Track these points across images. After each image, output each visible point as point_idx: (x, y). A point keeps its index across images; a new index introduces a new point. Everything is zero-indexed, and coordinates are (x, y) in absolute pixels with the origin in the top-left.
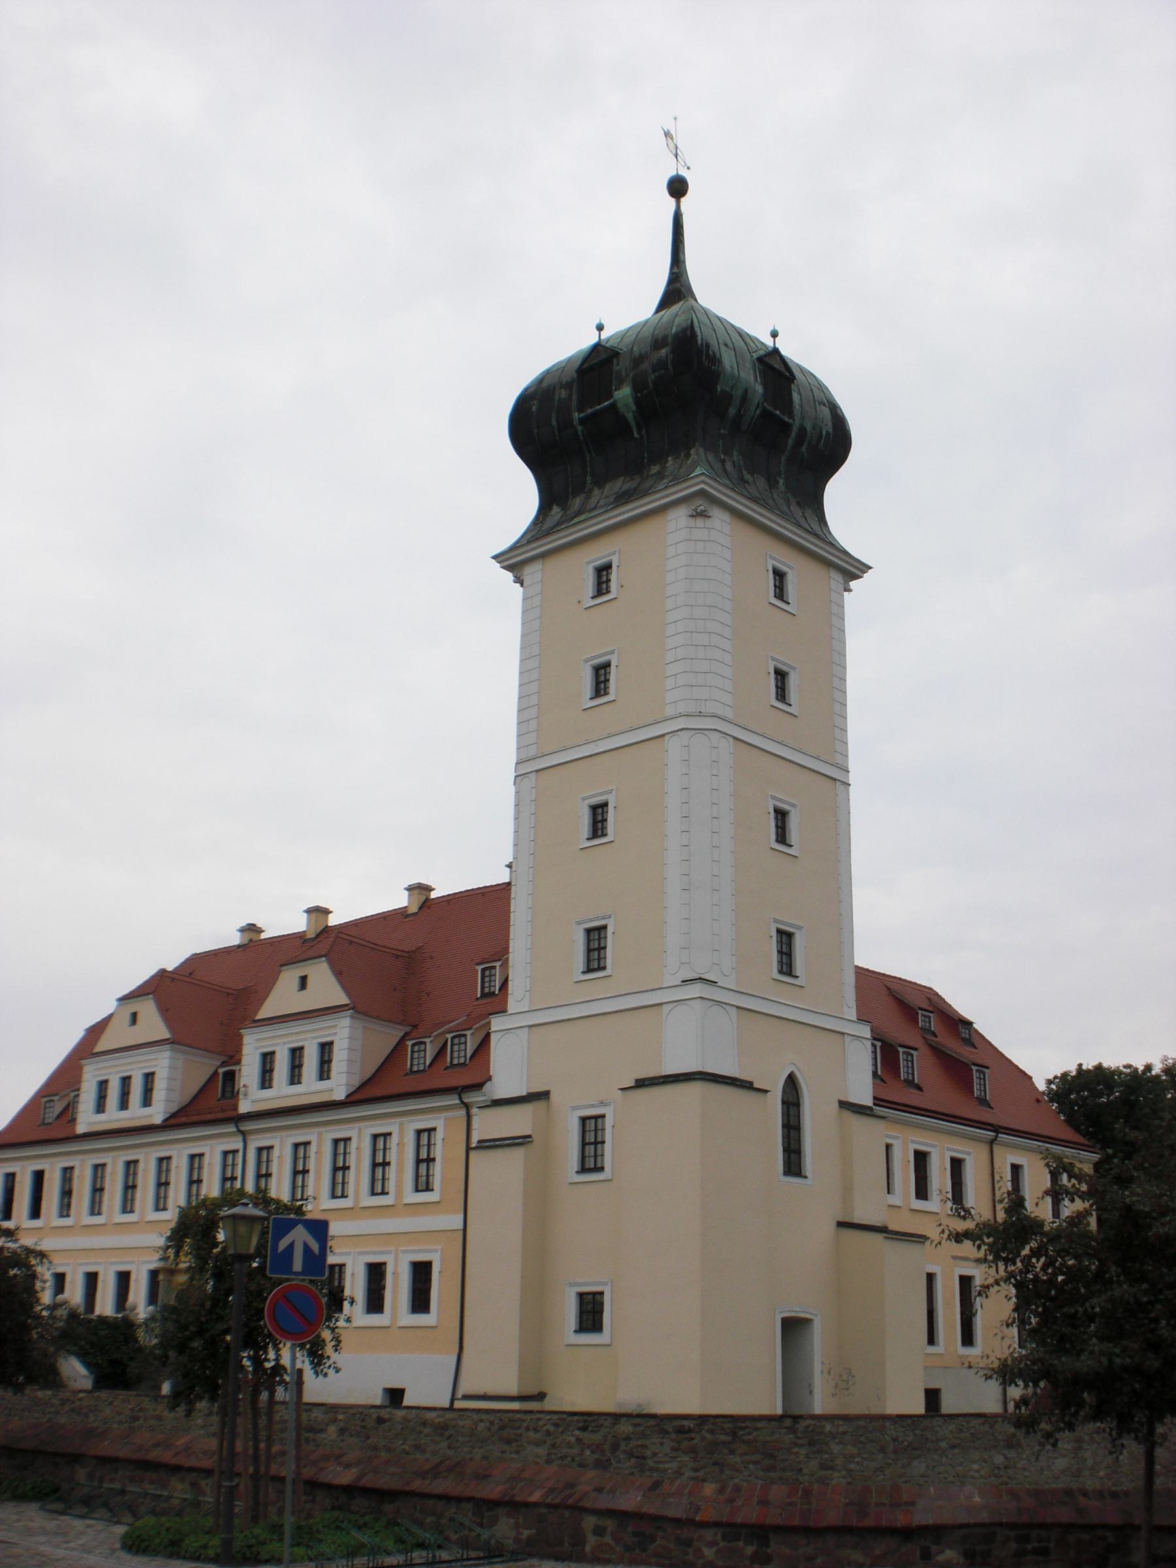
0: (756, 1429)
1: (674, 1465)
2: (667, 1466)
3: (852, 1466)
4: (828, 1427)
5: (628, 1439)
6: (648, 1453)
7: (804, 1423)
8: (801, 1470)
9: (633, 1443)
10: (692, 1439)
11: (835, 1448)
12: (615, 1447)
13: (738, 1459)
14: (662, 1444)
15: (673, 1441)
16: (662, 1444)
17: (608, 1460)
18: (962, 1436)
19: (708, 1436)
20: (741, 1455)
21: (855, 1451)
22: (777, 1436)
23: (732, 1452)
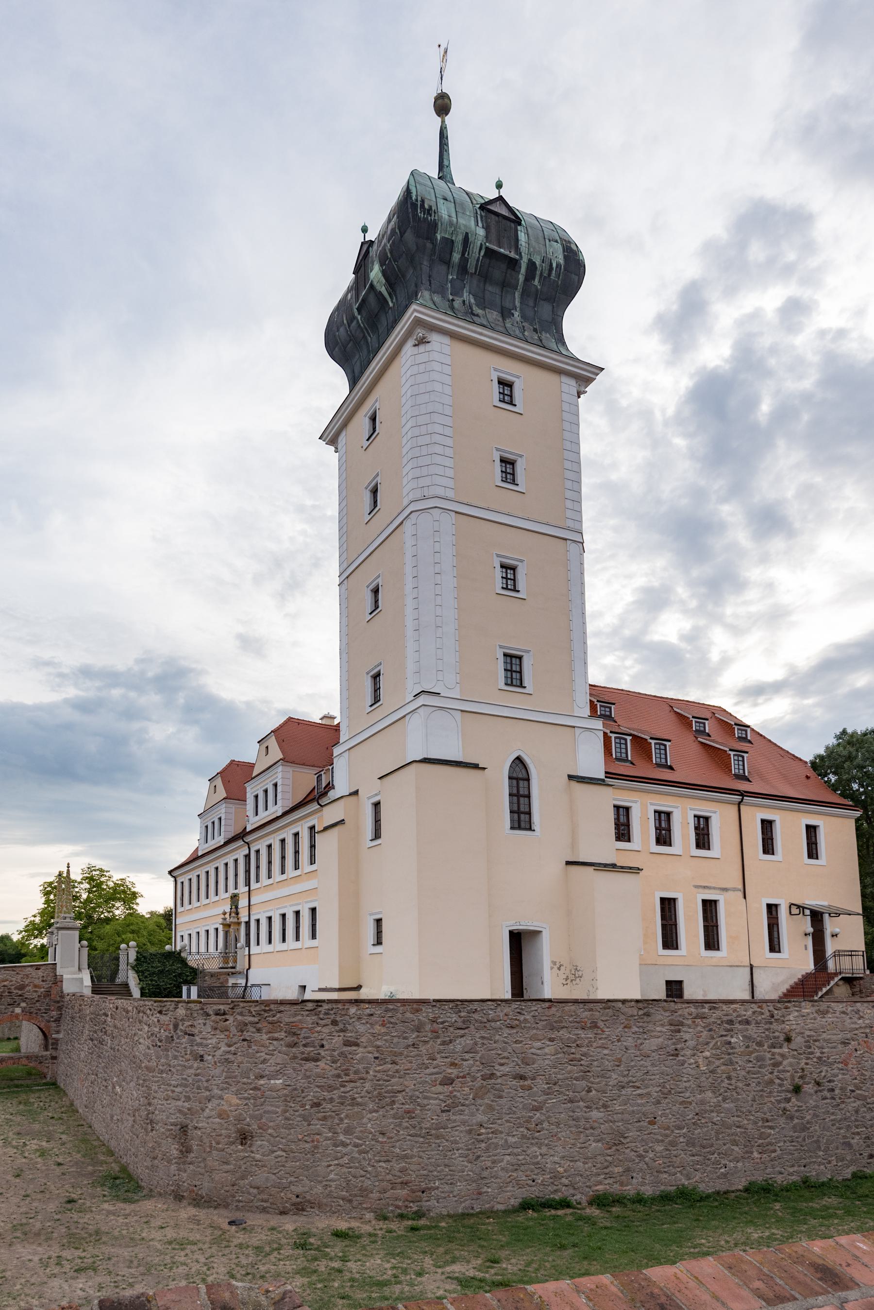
0: (280, 1012)
1: (214, 1041)
2: (209, 1041)
3: (379, 1043)
4: (353, 1010)
5: (183, 1020)
6: (196, 1031)
7: (326, 1006)
8: (322, 1046)
9: (187, 1023)
10: (226, 1020)
11: (361, 1028)
12: (176, 1027)
13: (265, 1037)
14: (205, 1024)
15: (213, 1021)
16: (205, 1024)
17: (172, 1037)
18: (522, 1018)
19: (239, 1018)
20: (267, 1033)
21: (383, 1030)
22: (300, 1017)
23: (259, 1030)
